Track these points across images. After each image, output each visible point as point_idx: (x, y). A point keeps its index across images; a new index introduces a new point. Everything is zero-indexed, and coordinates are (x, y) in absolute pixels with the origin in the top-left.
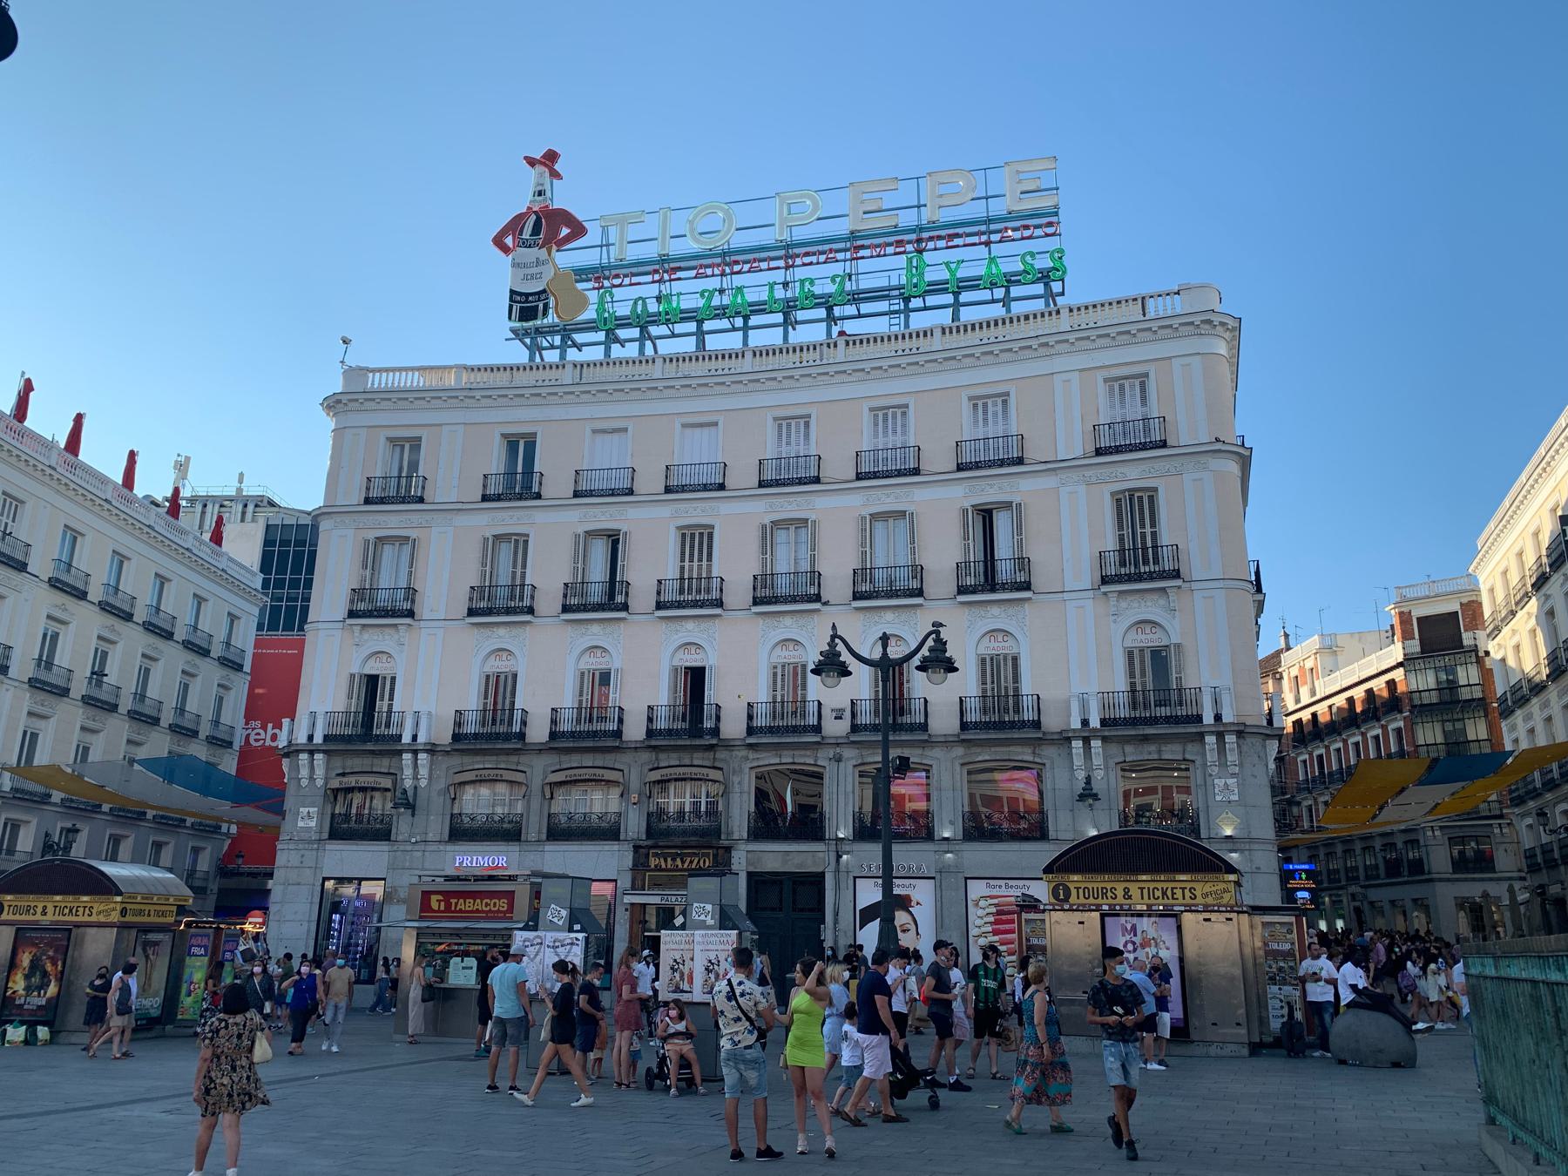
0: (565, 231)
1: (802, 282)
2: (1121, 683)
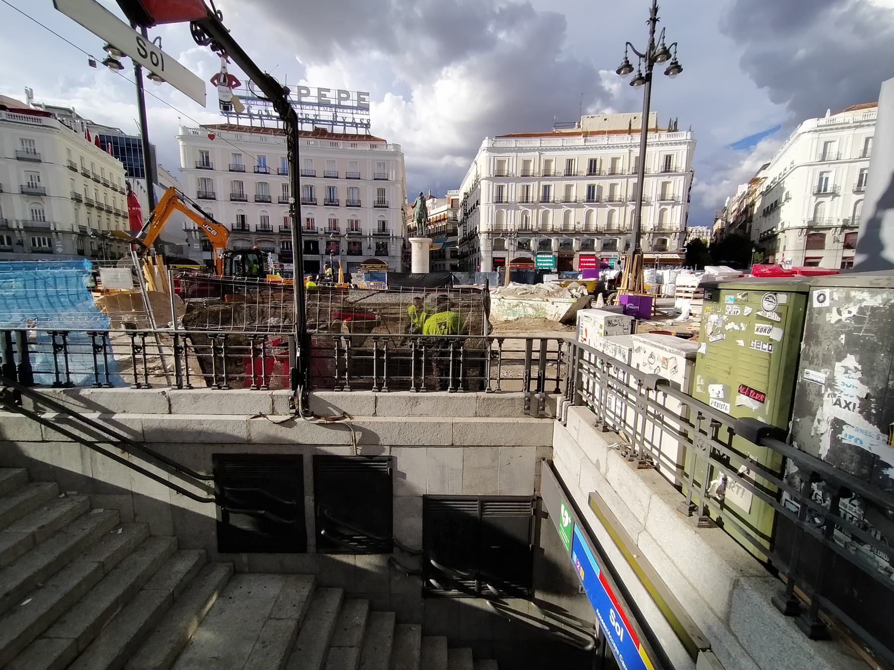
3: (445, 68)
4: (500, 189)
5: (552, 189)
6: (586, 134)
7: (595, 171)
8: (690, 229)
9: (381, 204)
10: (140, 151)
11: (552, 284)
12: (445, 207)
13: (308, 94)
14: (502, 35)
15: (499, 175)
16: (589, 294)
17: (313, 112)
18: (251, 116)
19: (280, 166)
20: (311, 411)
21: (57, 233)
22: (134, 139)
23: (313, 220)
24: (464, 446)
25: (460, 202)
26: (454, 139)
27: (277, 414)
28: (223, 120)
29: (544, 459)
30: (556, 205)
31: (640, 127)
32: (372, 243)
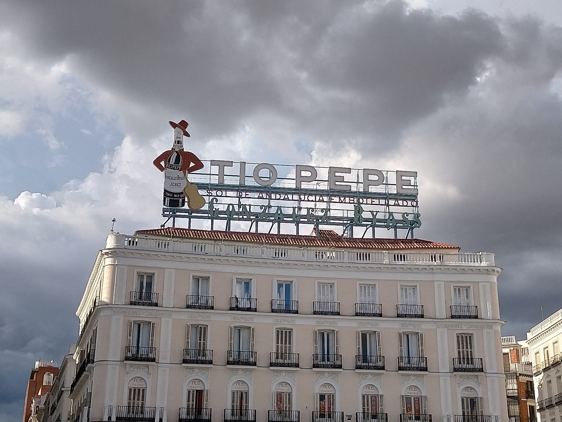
0: (192, 164)
1: (308, 209)
23: (332, 397)
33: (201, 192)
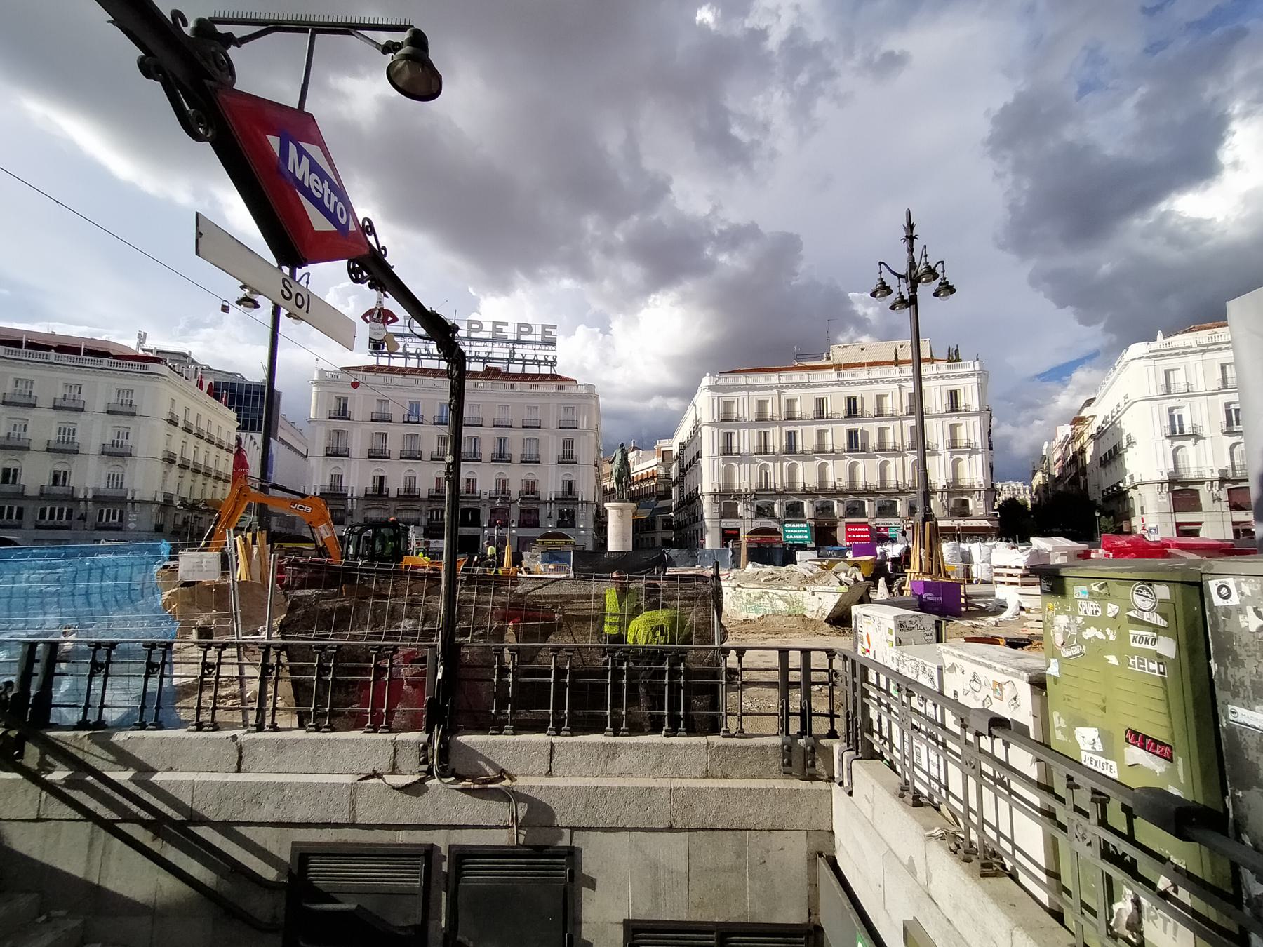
2: (560, 489)
3: (653, 296)
4: (728, 437)
5: (799, 436)
6: (838, 367)
7: (855, 412)
8: (999, 485)
9: (568, 459)
10: (262, 400)
11: (809, 565)
12: (654, 461)
13: (480, 329)
14: (723, 258)
15: (726, 418)
16: (866, 579)
17: (485, 349)
18: (406, 355)
19: (437, 413)
20: (451, 766)
21: (133, 503)
22: (256, 386)
23: (475, 481)
24: (690, 830)
25: (674, 454)
26: (665, 377)
27: (400, 773)
28: (371, 361)
29: (821, 855)
30: (805, 456)
31: (910, 357)
32: (554, 510)
33: (396, 339)
